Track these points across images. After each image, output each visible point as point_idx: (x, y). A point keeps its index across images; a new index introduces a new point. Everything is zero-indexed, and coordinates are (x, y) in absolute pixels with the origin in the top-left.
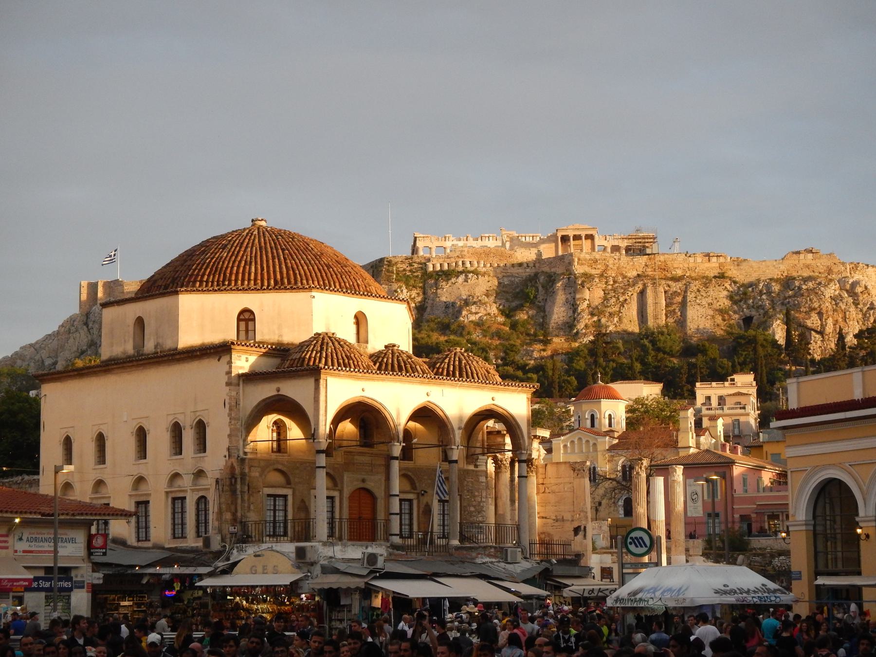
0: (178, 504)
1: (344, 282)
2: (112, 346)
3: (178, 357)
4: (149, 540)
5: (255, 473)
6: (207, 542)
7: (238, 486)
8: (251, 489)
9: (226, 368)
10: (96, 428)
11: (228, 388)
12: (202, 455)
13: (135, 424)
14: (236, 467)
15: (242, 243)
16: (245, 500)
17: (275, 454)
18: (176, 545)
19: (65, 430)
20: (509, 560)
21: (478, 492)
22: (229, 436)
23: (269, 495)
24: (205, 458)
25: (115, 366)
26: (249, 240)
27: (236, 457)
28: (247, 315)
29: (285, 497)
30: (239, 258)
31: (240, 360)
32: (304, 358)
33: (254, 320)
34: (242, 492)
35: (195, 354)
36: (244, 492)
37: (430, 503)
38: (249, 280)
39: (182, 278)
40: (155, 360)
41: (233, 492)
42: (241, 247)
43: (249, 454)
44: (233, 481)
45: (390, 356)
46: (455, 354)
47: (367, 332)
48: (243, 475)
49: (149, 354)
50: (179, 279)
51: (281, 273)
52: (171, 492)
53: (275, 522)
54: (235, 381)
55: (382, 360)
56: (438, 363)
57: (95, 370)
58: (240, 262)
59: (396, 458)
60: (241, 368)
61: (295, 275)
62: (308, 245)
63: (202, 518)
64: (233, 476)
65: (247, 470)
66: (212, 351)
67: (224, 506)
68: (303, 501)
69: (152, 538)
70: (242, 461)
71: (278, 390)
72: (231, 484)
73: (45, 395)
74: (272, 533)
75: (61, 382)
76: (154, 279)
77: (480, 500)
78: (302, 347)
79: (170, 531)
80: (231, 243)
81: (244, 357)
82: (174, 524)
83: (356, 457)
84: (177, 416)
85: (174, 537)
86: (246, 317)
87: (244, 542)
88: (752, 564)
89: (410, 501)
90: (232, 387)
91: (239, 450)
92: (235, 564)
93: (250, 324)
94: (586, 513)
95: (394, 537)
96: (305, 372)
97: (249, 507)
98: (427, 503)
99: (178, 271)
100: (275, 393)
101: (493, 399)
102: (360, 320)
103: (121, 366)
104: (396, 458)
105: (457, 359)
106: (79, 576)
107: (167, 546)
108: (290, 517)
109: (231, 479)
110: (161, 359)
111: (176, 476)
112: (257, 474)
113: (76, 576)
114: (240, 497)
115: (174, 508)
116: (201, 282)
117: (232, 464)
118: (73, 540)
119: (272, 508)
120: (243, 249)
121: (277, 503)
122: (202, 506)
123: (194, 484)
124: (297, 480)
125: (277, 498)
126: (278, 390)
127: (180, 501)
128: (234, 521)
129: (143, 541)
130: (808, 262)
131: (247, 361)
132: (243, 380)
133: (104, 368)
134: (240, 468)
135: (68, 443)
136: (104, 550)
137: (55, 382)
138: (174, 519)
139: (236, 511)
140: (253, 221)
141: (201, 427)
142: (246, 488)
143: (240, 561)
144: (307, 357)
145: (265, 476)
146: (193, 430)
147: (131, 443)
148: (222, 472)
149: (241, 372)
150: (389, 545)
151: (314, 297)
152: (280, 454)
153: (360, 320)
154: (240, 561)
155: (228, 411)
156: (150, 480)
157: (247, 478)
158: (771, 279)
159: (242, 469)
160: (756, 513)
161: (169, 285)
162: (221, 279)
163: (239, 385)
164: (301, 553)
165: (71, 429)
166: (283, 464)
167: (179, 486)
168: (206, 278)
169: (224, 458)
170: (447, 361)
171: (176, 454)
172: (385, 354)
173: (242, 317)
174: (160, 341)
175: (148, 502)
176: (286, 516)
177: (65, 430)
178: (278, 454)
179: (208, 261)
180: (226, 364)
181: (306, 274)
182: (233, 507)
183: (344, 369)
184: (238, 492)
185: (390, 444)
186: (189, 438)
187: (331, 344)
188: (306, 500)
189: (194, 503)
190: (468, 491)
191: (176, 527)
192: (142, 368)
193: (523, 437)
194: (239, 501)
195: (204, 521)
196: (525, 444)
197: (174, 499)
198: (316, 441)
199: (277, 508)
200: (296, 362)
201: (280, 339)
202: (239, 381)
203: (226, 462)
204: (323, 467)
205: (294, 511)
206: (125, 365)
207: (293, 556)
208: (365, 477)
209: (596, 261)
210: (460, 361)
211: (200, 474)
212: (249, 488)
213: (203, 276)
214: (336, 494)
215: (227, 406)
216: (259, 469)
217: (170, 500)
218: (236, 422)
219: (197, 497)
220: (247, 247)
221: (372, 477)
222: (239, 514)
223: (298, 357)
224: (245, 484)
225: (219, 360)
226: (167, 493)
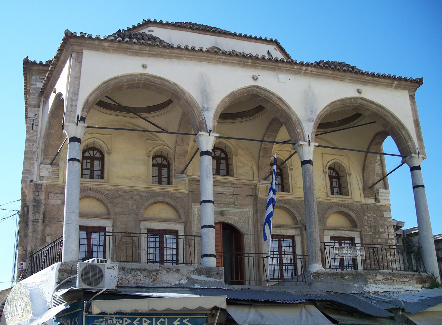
21: (384, 228)
27: (28, 180)
36: (37, 222)
44: (26, 209)
65: (42, 197)
70: (38, 187)
77: (387, 237)
89: (292, 238)
91: (32, 174)
95: (206, 259)
124: (117, 209)
134: (34, 194)
142: (41, 217)
150: (192, 269)
157: (43, 207)
163: (39, 106)
166: (97, 191)
190: (370, 227)
196: (414, 147)
202: (40, 102)
208: (224, 209)
212: (44, 217)
214: (179, 227)
218: (31, 144)
221: (235, 210)
224: (40, 213)
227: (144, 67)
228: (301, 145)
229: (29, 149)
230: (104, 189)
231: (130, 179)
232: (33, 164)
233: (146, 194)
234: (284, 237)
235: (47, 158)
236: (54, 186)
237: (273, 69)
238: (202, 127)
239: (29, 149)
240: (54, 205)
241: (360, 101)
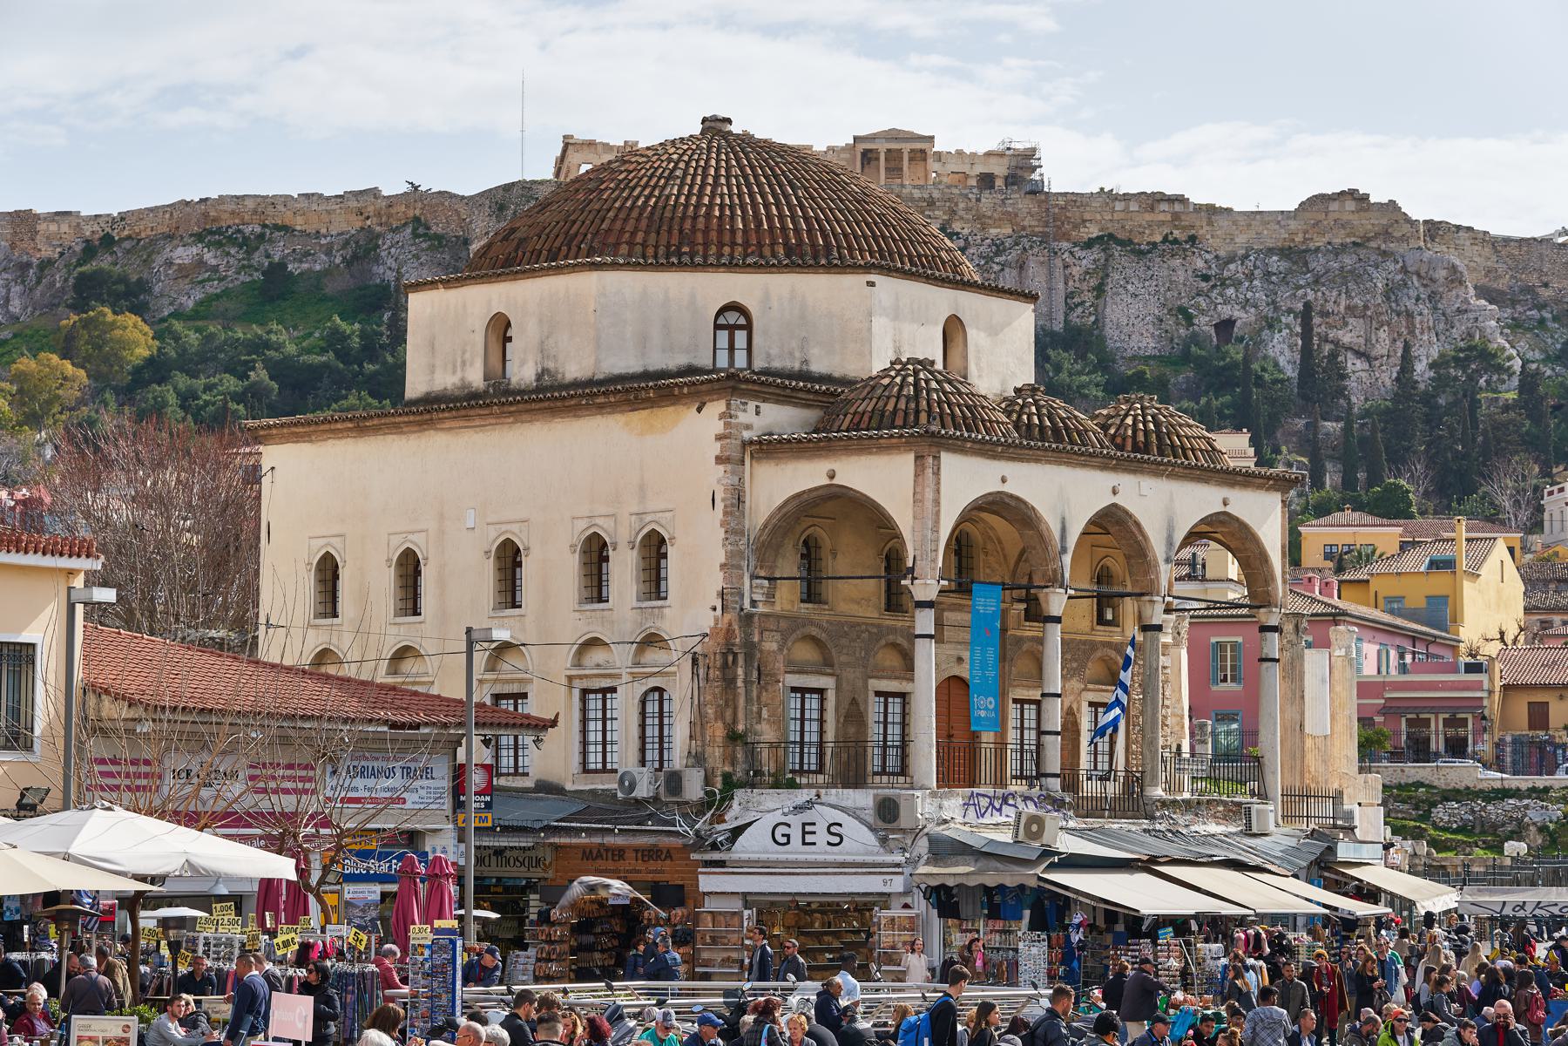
0: (594, 703)
1: (919, 256)
2: (433, 372)
3: (601, 400)
4: (527, 774)
5: (771, 645)
6: (674, 782)
7: (740, 671)
8: (763, 676)
9: (719, 427)
10: (396, 540)
11: (721, 468)
12: (660, 603)
13: (493, 534)
14: (737, 632)
15: (705, 169)
16: (752, 699)
17: (807, 605)
18: (593, 787)
19: (322, 542)
20: (1255, 830)
22: (723, 566)
23: (794, 689)
24: (666, 611)
25: (446, 415)
26: (718, 161)
28: (732, 318)
29: (821, 692)
30: (706, 200)
31: (745, 411)
32: (883, 412)
33: (748, 327)
34: (747, 682)
35: (643, 394)
36: (752, 682)
37: (1075, 707)
38: (733, 244)
39: (589, 236)
40: (546, 404)
41: (729, 682)
42: (705, 176)
43: (760, 605)
44: (730, 658)
45: (1034, 409)
46: (1143, 408)
47: (965, 358)
48: (750, 648)
49: (521, 392)
50: (580, 238)
51: (797, 230)
52: (581, 677)
53: (802, 743)
54: (736, 455)
55: (1019, 416)
56: (1111, 425)
57: (398, 419)
58: (711, 206)
59: (1058, 620)
60: (748, 427)
61: (825, 237)
62: (838, 175)
63: (652, 731)
64: (728, 651)
65: (756, 639)
66: (685, 390)
67: (710, 711)
68: (854, 702)
69: (530, 771)
70: (750, 616)
71: (832, 477)
72: (725, 666)
73: (273, 468)
74: (797, 767)
75: (311, 441)
76: (518, 235)
78: (873, 388)
79: (576, 759)
80: (682, 165)
81: (752, 405)
82: (585, 743)
83: (946, 614)
84: (599, 521)
85: (586, 771)
86: (734, 319)
87: (753, 786)
88: (1393, 815)
89: (1038, 703)
90: (729, 467)
91: (742, 596)
92: (737, 832)
93: (741, 337)
94: (1182, 717)
95: (1050, 780)
96: (894, 441)
97: (759, 713)
98: (1070, 708)
99: (574, 222)
100: (826, 481)
101: (1225, 504)
102: (953, 330)
103: (463, 412)
104: (1058, 620)
105: (1150, 418)
106: (439, 849)
107: (569, 787)
108: (830, 736)
109: (724, 655)
110: (559, 404)
111: (594, 643)
112: (774, 646)
113: (434, 851)
114: (741, 691)
115: (584, 710)
116: (631, 244)
117: (730, 625)
118: (427, 772)
119: (798, 716)
120: (710, 180)
121: (807, 706)
122: (652, 708)
123: (637, 664)
124: (843, 658)
125: (807, 696)
126: (832, 476)
127: (600, 696)
128: (733, 737)
129: (508, 774)
130: (1346, 217)
131: (758, 413)
132: (752, 457)
133: (418, 418)
135: (328, 572)
136: (488, 798)
137: (297, 442)
138: (584, 732)
139: (735, 721)
140: (704, 120)
141: (654, 548)
142: (755, 674)
143: (750, 824)
144: (890, 407)
145: (789, 650)
146: (635, 552)
147: (486, 576)
148: (707, 639)
149: (747, 435)
151: (871, 284)
152: (816, 606)
153: (953, 330)
154: (750, 824)
155: (721, 516)
156: (532, 656)
158: (1270, 251)
159: (748, 635)
160: (1384, 714)
161: (560, 249)
162: (675, 241)
163: (743, 462)
164: (888, 811)
165: (336, 541)
166: (819, 626)
167: (598, 665)
168: (640, 237)
169: (713, 613)
170: (1129, 421)
171: (590, 600)
172: (1022, 407)
173: (721, 321)
174: (551, 365)
175: (524, 696)
176: (822, 732)
177: (322, 542)
178: (810, 606)
179: (640, 203)
180: (717, 417)
181: (846, 235)
182: (728, 714)
183: (966, 435)
184: (740, 683)
185: (1045, 590)
186: (624, 569)
187: (934, 385)
188: (860, 700)
189: (636, 701)
191: (592, 748)
192: (511, 420)
193: (1273, 578)
194: (742, 701)
195: (657, 740)
196: (1276, 595)
197: (585, 692)
198: (916, 582)
199: (807, 716)
200: (866, 418)
201: (805, 368)
203: (716, 620)
204: (930, 636)
205: (838, 721)
206: (472, 412)
207: (870, 816)
209: (931, 203)
210: (1157, 423)
211: (651, 641)
213: (633, 234)
215: (720, 505)
216: (778, 636)
217: (576, 693)
219: (644, 689)
220: (717, 177)
222: (741, 727)
223: (870, 409)
225: (699, 410)
226: (570, 678)
227: (1004, 480)
228: (1152, 602)
229: (735, 548)
230: (827, 621)
231: (859, 603)
232: (742, 577)
233: (875, 630)
234: (1030, 702)
235: (761, 568)
236: (767, 616)
237: (1134, 472)
238: (1056, 580)
239: (735, 548)
240: (769, 652)
241: (1222, 518)
